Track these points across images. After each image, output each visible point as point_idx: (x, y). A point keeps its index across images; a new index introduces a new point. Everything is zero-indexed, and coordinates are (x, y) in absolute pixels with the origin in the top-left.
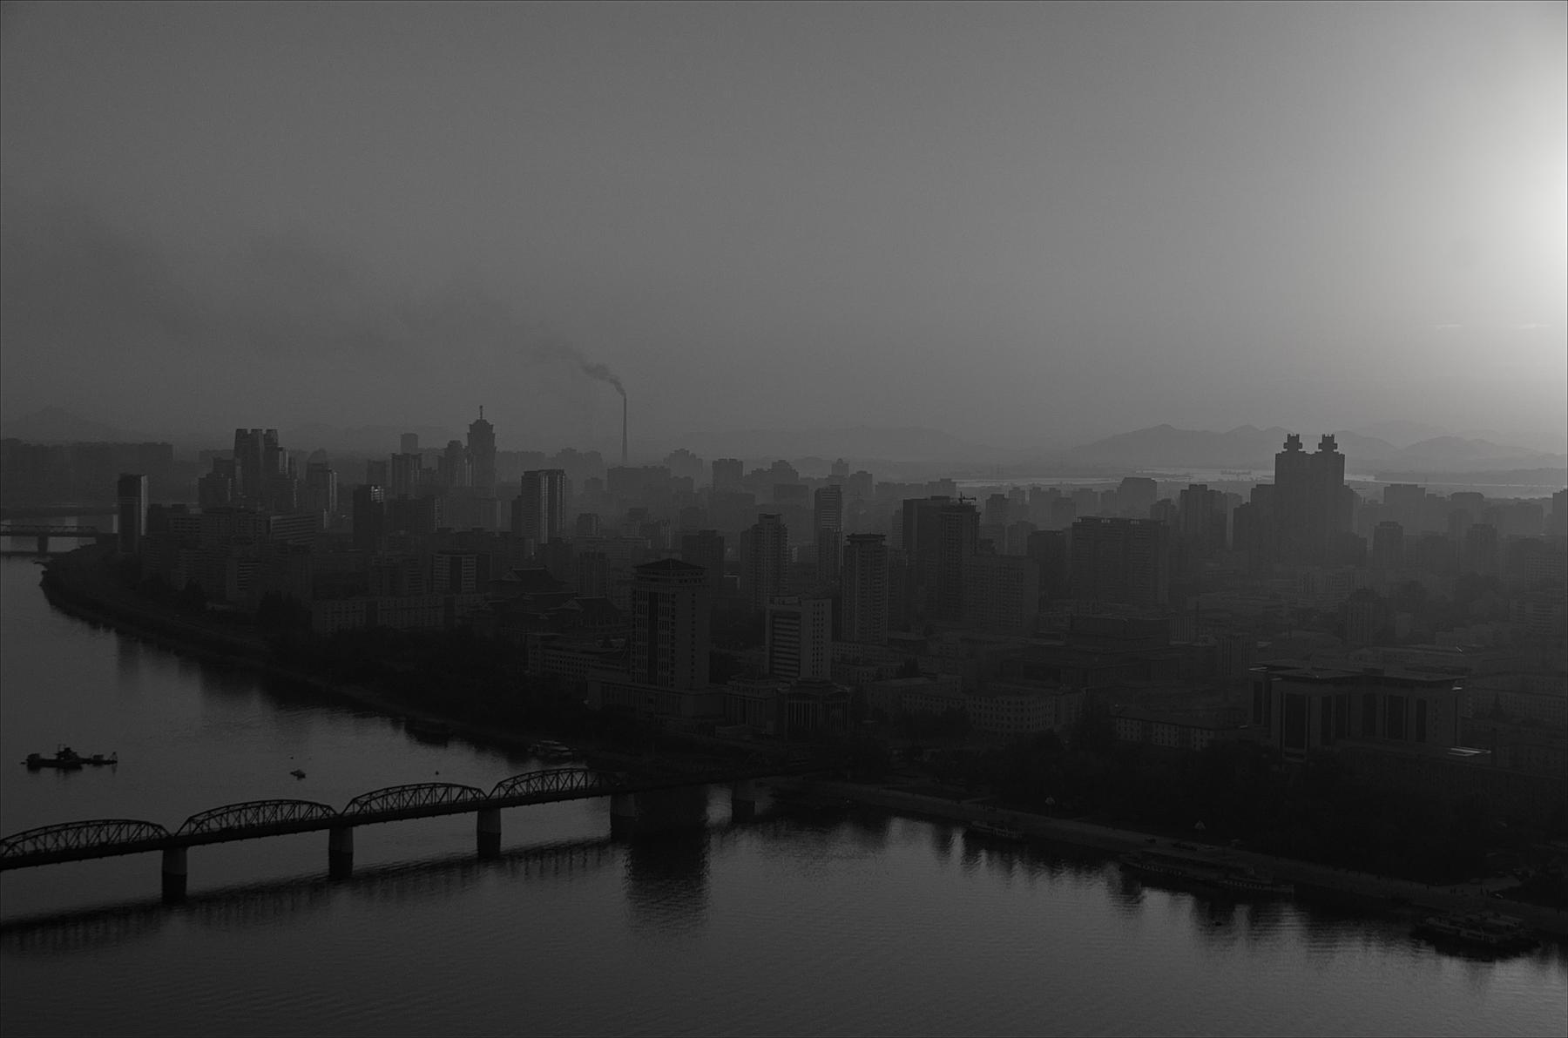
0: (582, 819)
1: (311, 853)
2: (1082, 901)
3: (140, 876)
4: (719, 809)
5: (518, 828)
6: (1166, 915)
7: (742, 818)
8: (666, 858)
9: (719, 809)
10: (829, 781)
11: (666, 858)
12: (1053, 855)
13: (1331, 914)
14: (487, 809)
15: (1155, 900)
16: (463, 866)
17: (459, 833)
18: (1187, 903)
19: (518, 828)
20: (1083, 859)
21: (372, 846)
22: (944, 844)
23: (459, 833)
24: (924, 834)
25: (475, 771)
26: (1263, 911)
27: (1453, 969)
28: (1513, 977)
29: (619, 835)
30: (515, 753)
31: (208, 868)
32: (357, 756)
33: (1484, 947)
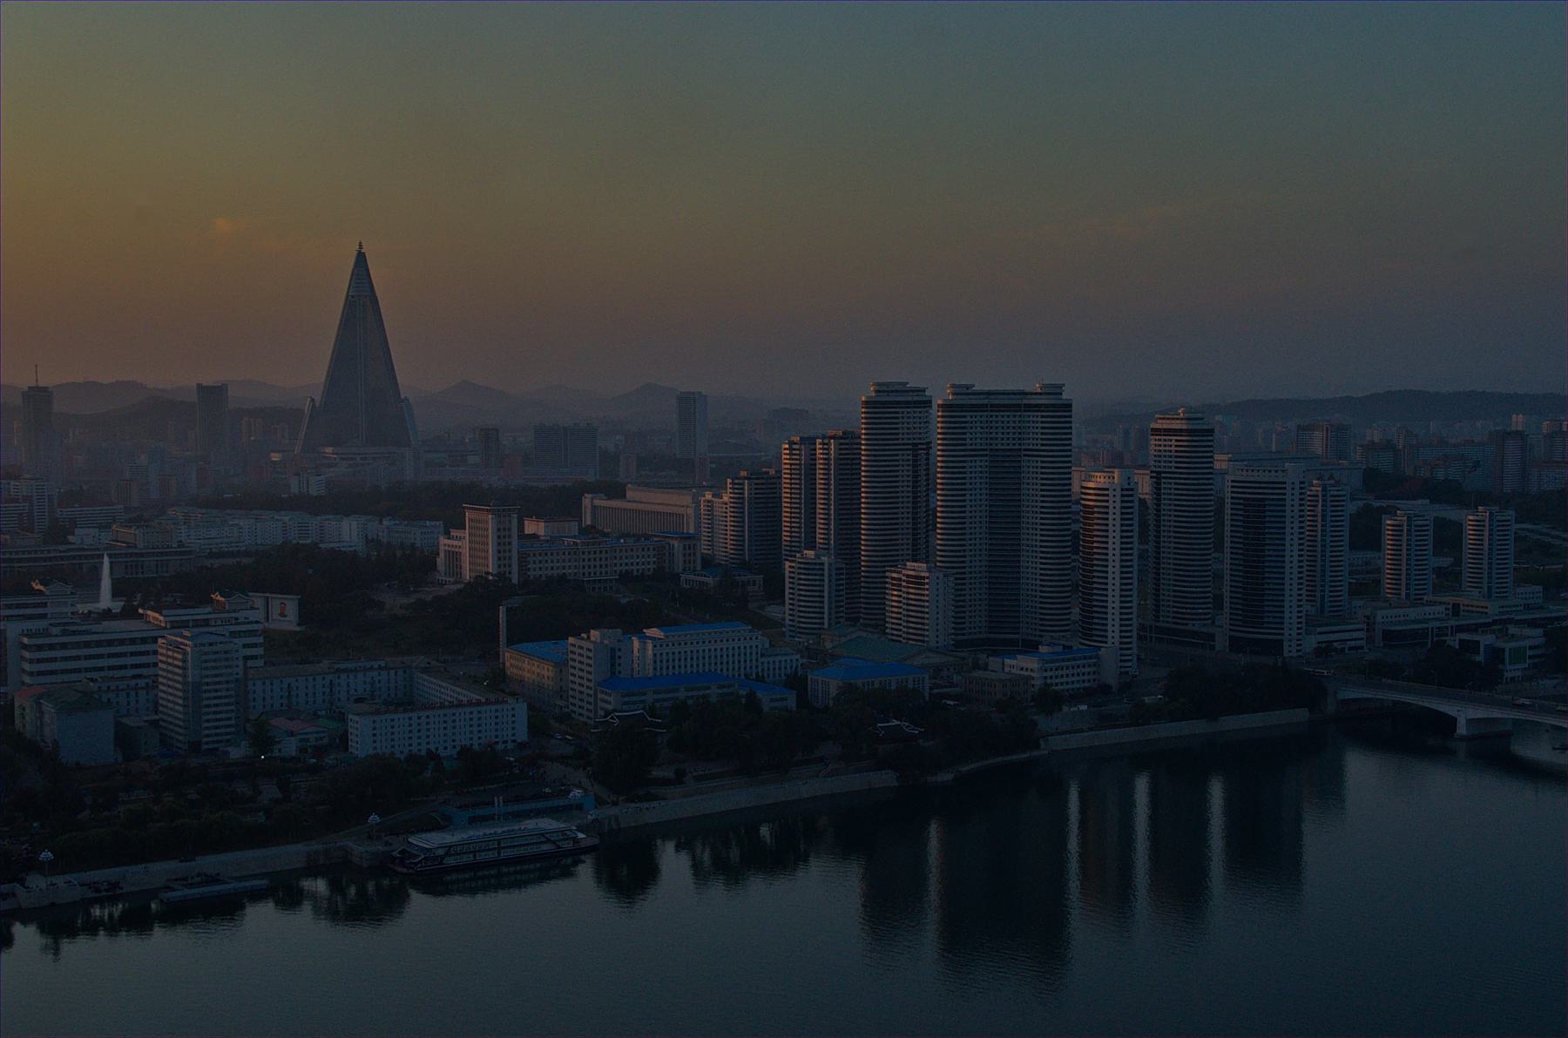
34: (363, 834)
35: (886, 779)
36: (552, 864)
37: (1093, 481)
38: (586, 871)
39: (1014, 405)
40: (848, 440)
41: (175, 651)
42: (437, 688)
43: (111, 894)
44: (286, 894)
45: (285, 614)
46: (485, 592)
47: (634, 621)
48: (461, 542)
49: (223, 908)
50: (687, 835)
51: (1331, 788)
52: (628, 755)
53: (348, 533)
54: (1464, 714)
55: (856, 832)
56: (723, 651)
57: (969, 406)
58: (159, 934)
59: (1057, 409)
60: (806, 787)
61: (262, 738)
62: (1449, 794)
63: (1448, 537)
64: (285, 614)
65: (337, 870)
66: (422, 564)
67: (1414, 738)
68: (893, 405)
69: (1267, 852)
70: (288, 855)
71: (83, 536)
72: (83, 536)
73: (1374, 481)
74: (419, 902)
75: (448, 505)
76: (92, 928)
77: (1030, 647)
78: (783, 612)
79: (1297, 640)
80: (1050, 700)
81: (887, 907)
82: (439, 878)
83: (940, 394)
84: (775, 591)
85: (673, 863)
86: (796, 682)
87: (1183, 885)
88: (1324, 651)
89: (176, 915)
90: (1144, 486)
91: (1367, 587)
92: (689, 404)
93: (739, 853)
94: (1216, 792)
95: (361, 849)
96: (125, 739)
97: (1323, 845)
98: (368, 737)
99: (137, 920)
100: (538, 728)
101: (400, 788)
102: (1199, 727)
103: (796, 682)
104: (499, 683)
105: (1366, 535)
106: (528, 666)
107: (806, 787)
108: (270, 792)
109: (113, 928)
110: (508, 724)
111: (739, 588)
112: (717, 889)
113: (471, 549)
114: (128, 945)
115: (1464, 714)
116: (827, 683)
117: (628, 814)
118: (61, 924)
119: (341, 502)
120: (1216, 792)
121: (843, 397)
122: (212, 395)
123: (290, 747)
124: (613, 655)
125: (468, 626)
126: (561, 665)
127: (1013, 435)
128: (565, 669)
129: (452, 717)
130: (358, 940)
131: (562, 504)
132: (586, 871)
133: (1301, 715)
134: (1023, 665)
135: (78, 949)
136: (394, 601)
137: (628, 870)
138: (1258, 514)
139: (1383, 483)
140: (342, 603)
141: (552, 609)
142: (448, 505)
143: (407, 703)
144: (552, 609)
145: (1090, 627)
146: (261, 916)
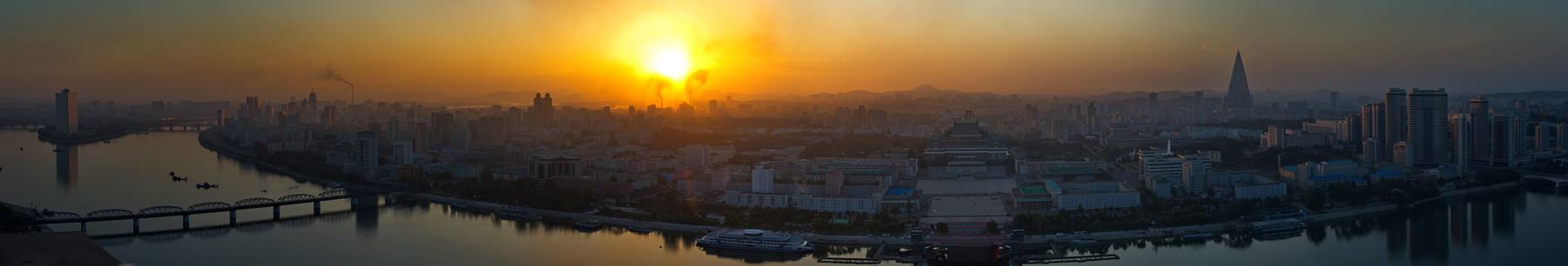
0: (344, 204)
1: (268, 213)
2: (484, 224)
3: (224, 218)
4: (381, 202)
5: (325, 207)
6: (508, 226)
7: (388, 204)
8: (366, 215)
9: (381, 202)
10: (412, 194)
11: (366, 215)
12: (476, 212)
13: (551, 224)
14: (316, 201)
15: (504, 222)
16: (310, 217)
17: (308, 208)
18: (513, 223)
19: (325, 207)
20: (484, 212)
21: (285, 211)
22: (445, 210)
23: (308, 208)
24: (440, 207)
25: (315, 191)
26: (534, 226)
27: (583, 234)
28: (597, 235)
29: (354, 208)
30: (324, 186)
31: (242, 216)
32: (278, 186)
33: (589, 229)
34: (1240, 222)
35: (1393, 206)
36: (1295, 232)
37: (1454, 117)
38: (1304, 234)
39: (1431, 94)
40: (1381, 105)
41: (1186, 166)
42: (1261, 179)
43: (1170, 234)
44: (1218, 240)
45: (1217, 157)
46: (1275, 151)
47: (1318, 159)
48: (1267, 136)
49: (1201, 241)
50: (1334, 223)
51: (1523, 204)
52: (1318, 199)
53: (1235, 133)
54: (1558, 181)
55: (1385, 223)
56: (1345, 168)
57: (1417, 95)
58: (1183, 247)
59: (1443, 95)
60: (1370, 209)
61: (1211, 193)
62: (1554, 203)
63: (1553, 132)
64: (1217, 157)
65: (1232, 232)
66: (1255, 143)
67: (1544, 188)
68: (1395, 95)
69: (1505, 224)
70: (1218, 226)
71: (1163, 134)
72: (1163, 134)
73: (1535, 117)
74: (1255, 241)
75: (1263, 125)
76: (1166, 244)
77: (1436, 166)
78: (1362, 157)
79: (1512, 162)
80: (1442, 182)
81: (1394, 245)
82: (1261, 235)
83: (1409, 91)
84: (1360, 151)
85: (1330, 232)
86: (1367, 178)
87: (1481, 235)
88: (1520, 165)
89: (1188, 242)
90: (1469, 119)
91: (1531, 146)
92: (1334, 94)
93: (1350, 229)
94: (1491, 207)
95: (1239, 226)
96: (1173, 191)
97: (1521, 221)
98: (1241, 193)
99: (1177, 243)
100: (1290, 191)
101: (1249, 209)
102: (1485, 188)
103: (1367, 178)
104: (1278, 178)
105: (1531, 132)
106: (1286, 173)
107: (1370, 209)
108: (1213, 208)
109: (1171, 244)
110: (1282, 190)
111: (1350, 150)
112: (1344, 240)
113: (1270, 138)
114: (1175, 249)
115: (1558, 181)
116: (1376, 178)
117: (1316, 217)
118: (1158, 242)
119: (1233, 124)
120: (1491, 207)
121: (1380, 93)
122: (1199, 94)
123: (1218, 195)
124: (1312, 170)
125: (1269, 161)
126: (1297, 172)
127: (1430, 103)
128: (1298, 174)
129: (1265, 187)
130: (1239, 253)
131: (1296, 125)
132: (1304, 234)
133: (1513, 184)
134: (1435, 171)
135: (1162, 249)
136: (1248, 153)
137: (1317, 234)
138: (1501, 126)
139: (1535, 117)
140: (1234, 153)
141: (1294, 156)
142: (1263, 125)
143: (1252, 183)
144: (1294, 156)
145: (1454, 160)
146: (1210, 244)
